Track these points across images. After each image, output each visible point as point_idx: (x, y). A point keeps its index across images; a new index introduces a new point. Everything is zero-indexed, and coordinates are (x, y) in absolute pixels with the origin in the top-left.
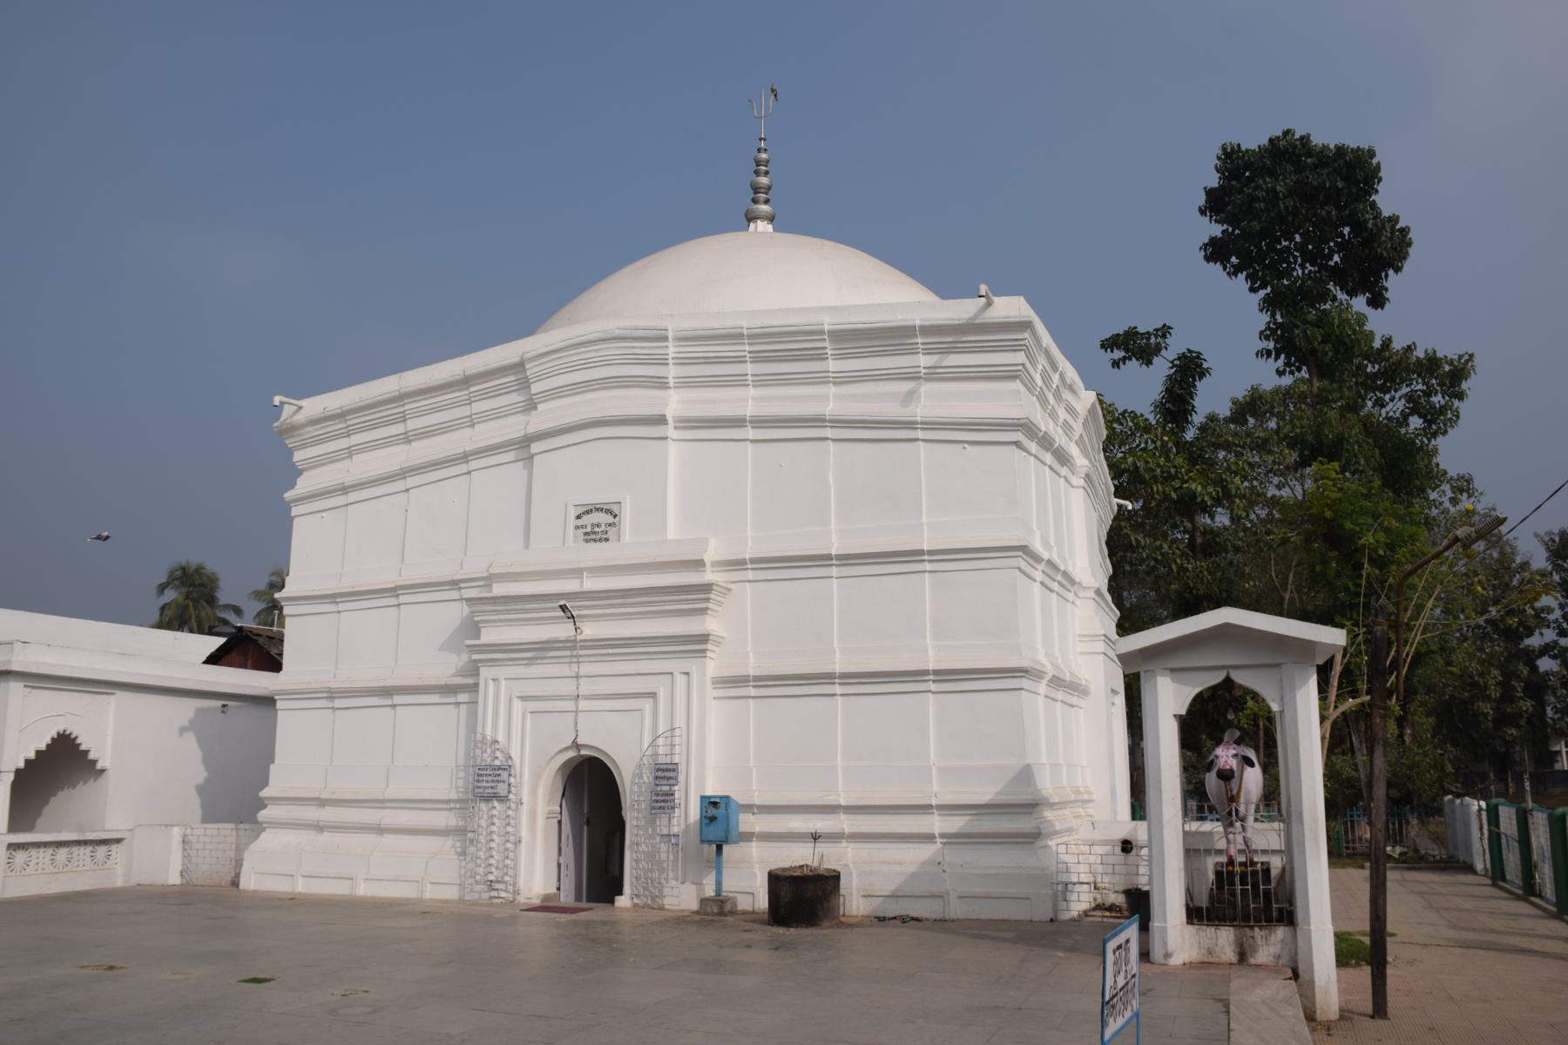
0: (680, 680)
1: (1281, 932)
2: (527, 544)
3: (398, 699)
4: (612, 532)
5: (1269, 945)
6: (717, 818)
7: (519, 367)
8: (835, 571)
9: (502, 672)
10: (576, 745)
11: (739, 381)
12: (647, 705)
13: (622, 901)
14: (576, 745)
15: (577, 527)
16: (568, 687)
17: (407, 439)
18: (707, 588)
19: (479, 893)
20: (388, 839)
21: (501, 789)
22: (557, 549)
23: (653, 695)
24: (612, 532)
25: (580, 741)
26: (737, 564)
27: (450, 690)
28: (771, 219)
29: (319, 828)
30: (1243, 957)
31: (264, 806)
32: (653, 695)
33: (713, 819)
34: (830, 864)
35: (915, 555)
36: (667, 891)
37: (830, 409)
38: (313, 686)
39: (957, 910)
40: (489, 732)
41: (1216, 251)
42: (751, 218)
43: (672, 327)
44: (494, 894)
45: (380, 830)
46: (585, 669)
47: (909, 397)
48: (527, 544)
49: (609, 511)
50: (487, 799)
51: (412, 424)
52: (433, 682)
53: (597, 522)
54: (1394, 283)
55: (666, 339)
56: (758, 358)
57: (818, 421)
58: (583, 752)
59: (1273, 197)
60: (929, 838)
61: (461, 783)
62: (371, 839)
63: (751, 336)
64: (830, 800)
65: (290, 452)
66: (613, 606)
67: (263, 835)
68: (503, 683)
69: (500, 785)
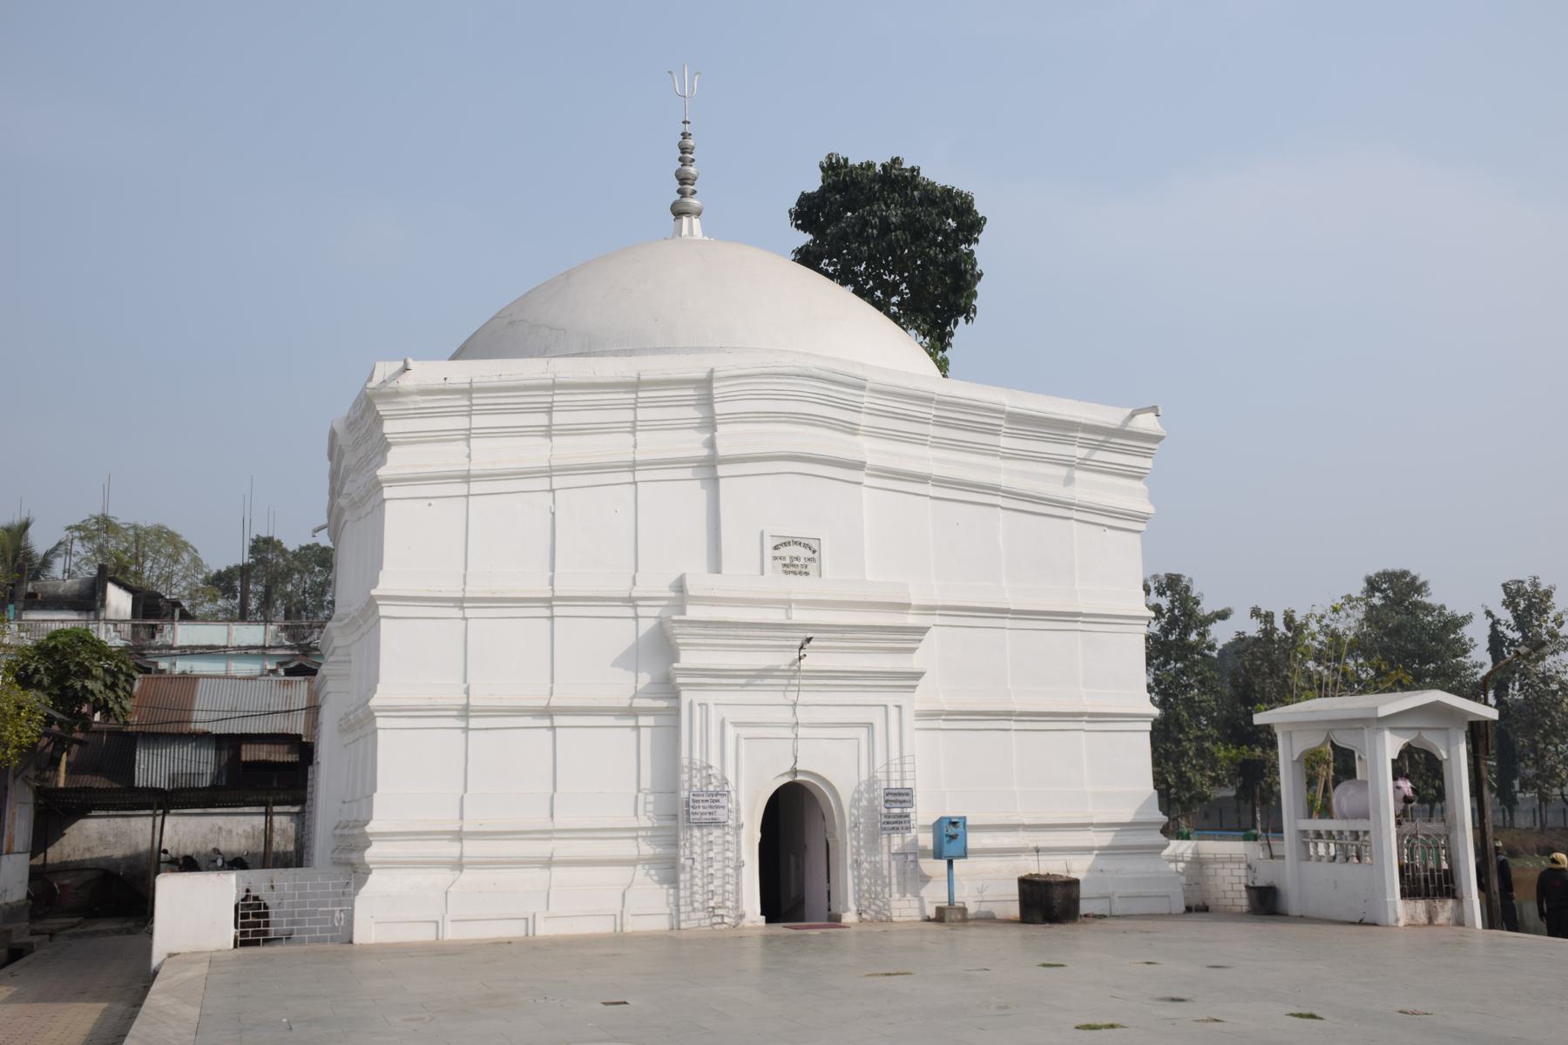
0: (893, 712)
1: (1450, 903)
2: (716, 567)
3: (558, 720)
4: (812, 567)
5: (1445, 909)
6: (950, 838)
7: (707, 383)
8: (1007, 623)
9: (711, 697)
10: (795, 772)
11: (919, 439)
12: (862, 733)
13: (849, 917)
14: (795, 772)
15: (775, 558)
16: (785, 715)
17: (548, 432)
18: (923, 630)
19: (695, 921)
20: (558, 873)
21: (721, 815)
22: (747, 578)
23: (870, 726)
24: (812, 567)
25: (799, 767)
26: (929, 609)
27: (631, 712)
28: (698, 214)
29: (459, 865)
30: (1431, 921)
31: (368, 845)
32: (870, 726)
33: (953, 837)
34: (1073, 876)
35: (1074, 615)
36: (894, 904)
37: (1004, 481)
38: (440, 702)
39: (1119, 908)
40: (697, 756)
41: (806, 257)
42: (678, 212)
43: (875, 379)
44: (716, 920)
45: (549, 863)
46: (804, 698)
47: (1069, 481)
48: (716, 567)
49: (806, 546)
50: (700, 825)
51: (558, 418)
52: (614, 704)
53: (797, 555)
54: (962, 332)
55: (862, 388)
56: (941, 423)
57: (994, 490)
58: (799, 778)
59: (885, 226)
60: (1089, 850)
61: (650, 807)
62: (537, 875)
63: (938, 402)
64: (1015, 820)
65: (379, 420)
66: (829, 639)
67: (372, 878)
68: (712, 709)
69: (720, 811)
